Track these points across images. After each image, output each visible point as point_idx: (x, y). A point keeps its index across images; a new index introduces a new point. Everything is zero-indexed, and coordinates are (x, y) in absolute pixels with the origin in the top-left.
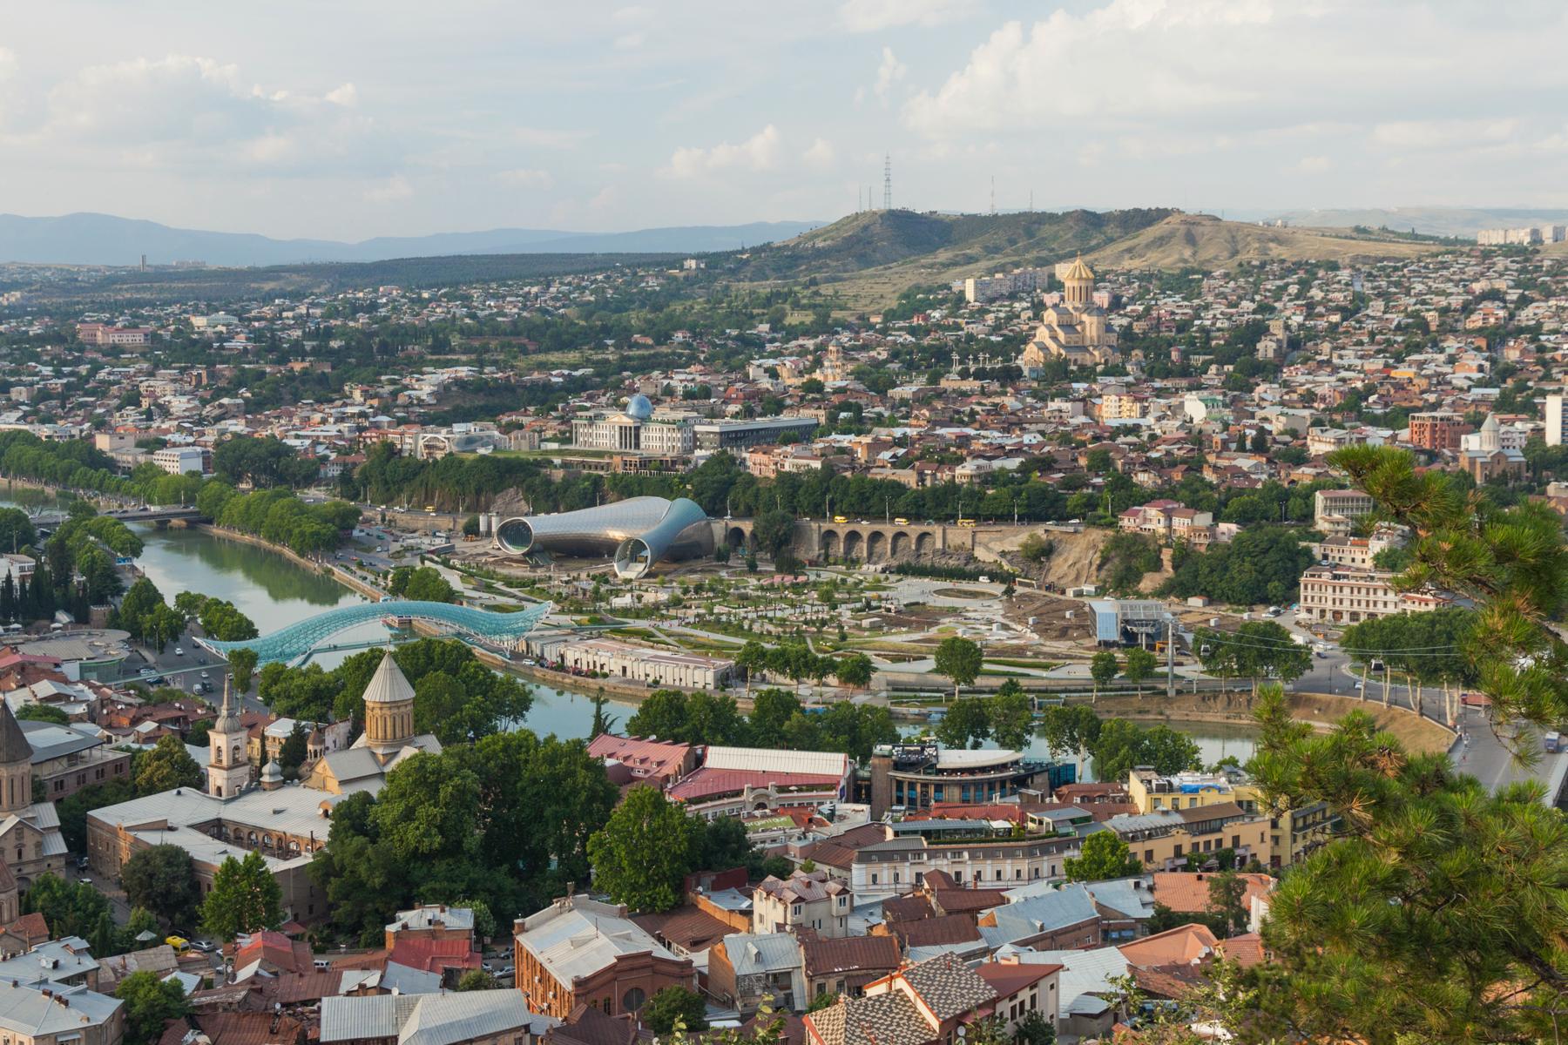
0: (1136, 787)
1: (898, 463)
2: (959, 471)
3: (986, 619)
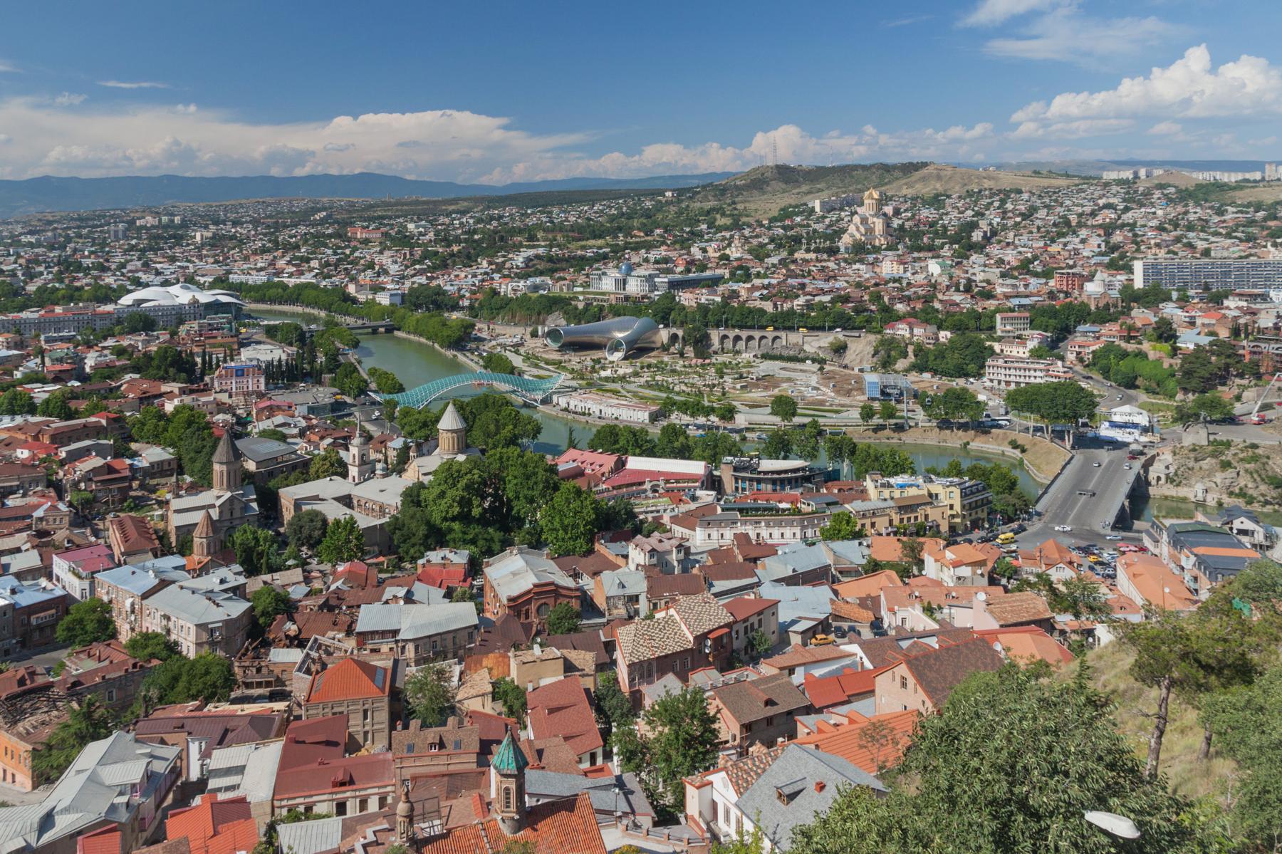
0: (869, 484)
1: (763, 298)
2: (796, 302)
3: (806, 384)
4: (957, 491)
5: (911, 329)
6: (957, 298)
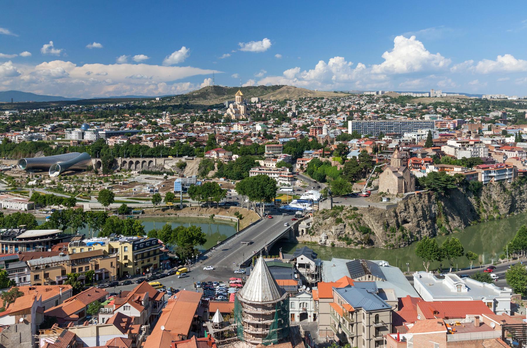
2: (165, 142)
4: (130, 247)
5: (218, 154)
6: (253, 139)
